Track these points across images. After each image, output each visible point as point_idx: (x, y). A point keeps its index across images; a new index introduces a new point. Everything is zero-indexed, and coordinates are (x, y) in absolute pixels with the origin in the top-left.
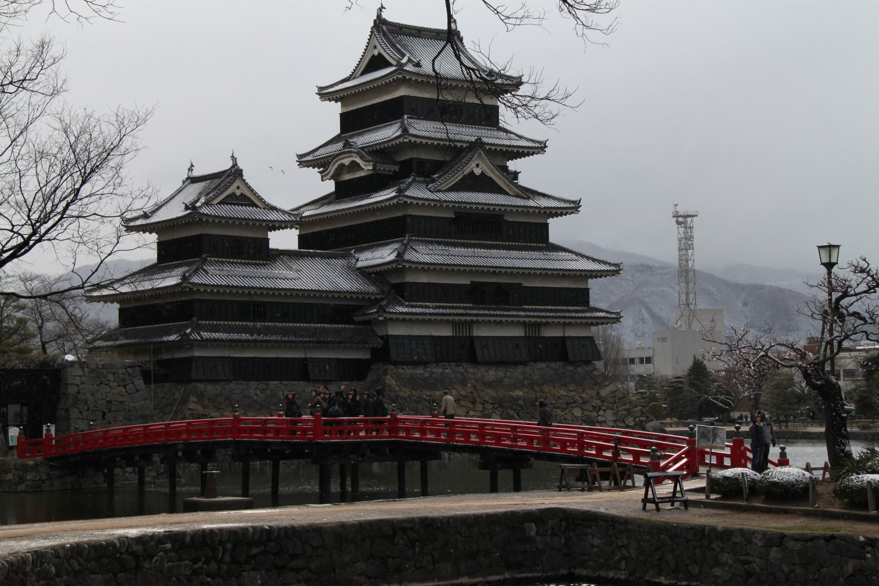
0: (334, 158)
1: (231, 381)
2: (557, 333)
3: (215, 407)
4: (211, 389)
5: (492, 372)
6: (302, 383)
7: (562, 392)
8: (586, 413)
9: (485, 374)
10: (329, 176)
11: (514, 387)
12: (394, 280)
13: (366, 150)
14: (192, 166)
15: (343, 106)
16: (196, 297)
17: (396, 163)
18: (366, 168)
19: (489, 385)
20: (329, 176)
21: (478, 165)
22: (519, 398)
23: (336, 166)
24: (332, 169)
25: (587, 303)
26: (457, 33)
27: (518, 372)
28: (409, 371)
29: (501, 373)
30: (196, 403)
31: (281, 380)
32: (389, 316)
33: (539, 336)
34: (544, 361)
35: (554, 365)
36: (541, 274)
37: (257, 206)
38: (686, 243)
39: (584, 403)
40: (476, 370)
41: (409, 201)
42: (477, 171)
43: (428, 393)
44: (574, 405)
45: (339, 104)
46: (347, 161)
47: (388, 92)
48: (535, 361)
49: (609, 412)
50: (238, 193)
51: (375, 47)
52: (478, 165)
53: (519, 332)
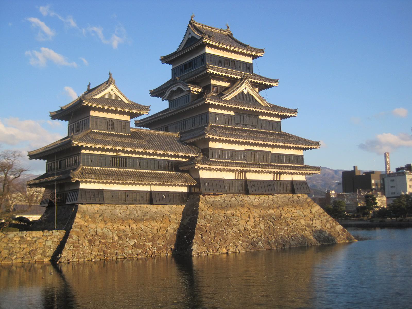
0: (168, 88)
5: (257, 200)
6: (149, 206)
9: (253, 201)
10: (166, 98)
12: (202, 147)
13: (186, 81)
14: (90, 84)
15: (173, 66)
18: (185, 90)
19: (256, 207)
20: (166, 98)
22: (272, 214)
23: (169, 92)
24: (167, 94)
25: (302, 163)
30: (80, 218)
31: (136, 204)
32: (200, 166)
33: (280, 180)
39: (305, 216)
42: (246, 92)
44: (300, 217)
45: (171, 65)
46: (175, 89)
47: (198, 53)
49: (318, 221)
51: (190, 34)
52: (245, 88)
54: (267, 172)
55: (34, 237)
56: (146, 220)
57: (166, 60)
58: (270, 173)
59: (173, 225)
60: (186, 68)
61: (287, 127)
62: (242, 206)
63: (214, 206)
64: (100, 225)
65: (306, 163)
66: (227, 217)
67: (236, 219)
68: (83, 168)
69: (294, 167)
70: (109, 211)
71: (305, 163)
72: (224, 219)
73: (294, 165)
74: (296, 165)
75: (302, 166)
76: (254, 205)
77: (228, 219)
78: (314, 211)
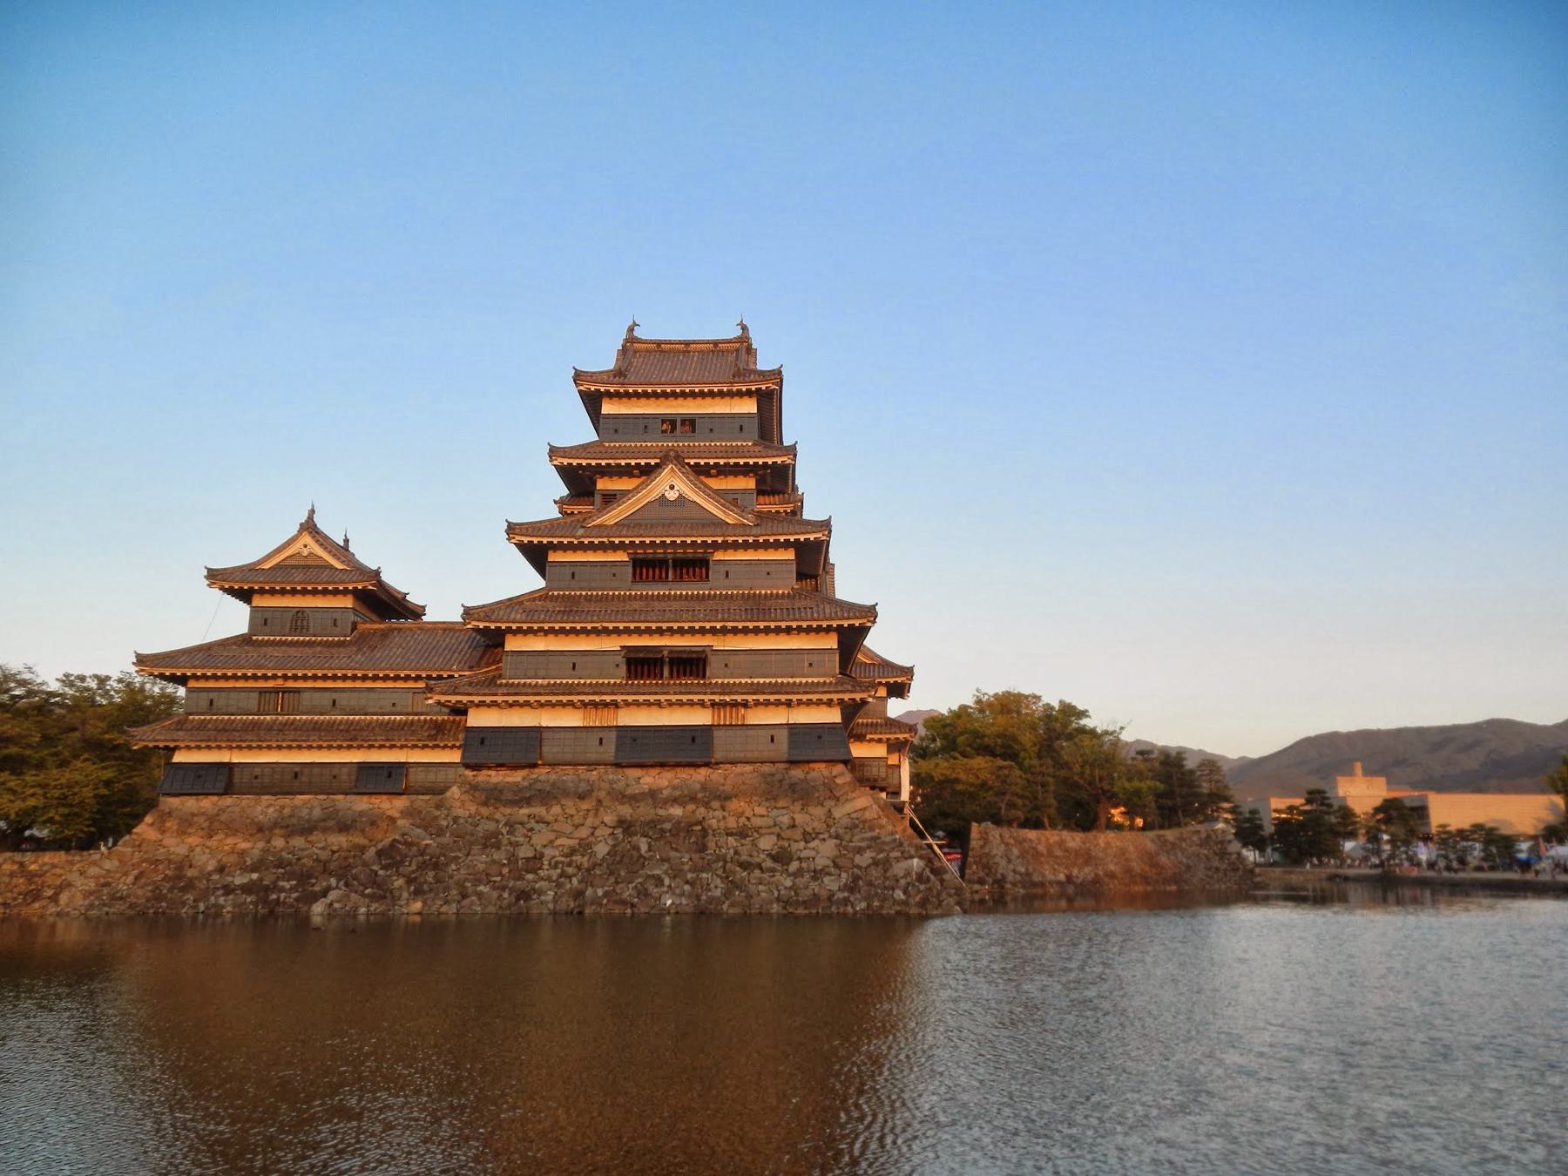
4: (190, 804)
7: (758, 810)
11: (675, 801)
21: (672, 487)
22: (668, 819)
28: (495, 777)
32: (443, 699)
42: (672, 496)
53: (702, 718)
56: (325, 830)
63: (493, 796)
70: (237, 809)
76: (629, 791)
78: (837, 813)
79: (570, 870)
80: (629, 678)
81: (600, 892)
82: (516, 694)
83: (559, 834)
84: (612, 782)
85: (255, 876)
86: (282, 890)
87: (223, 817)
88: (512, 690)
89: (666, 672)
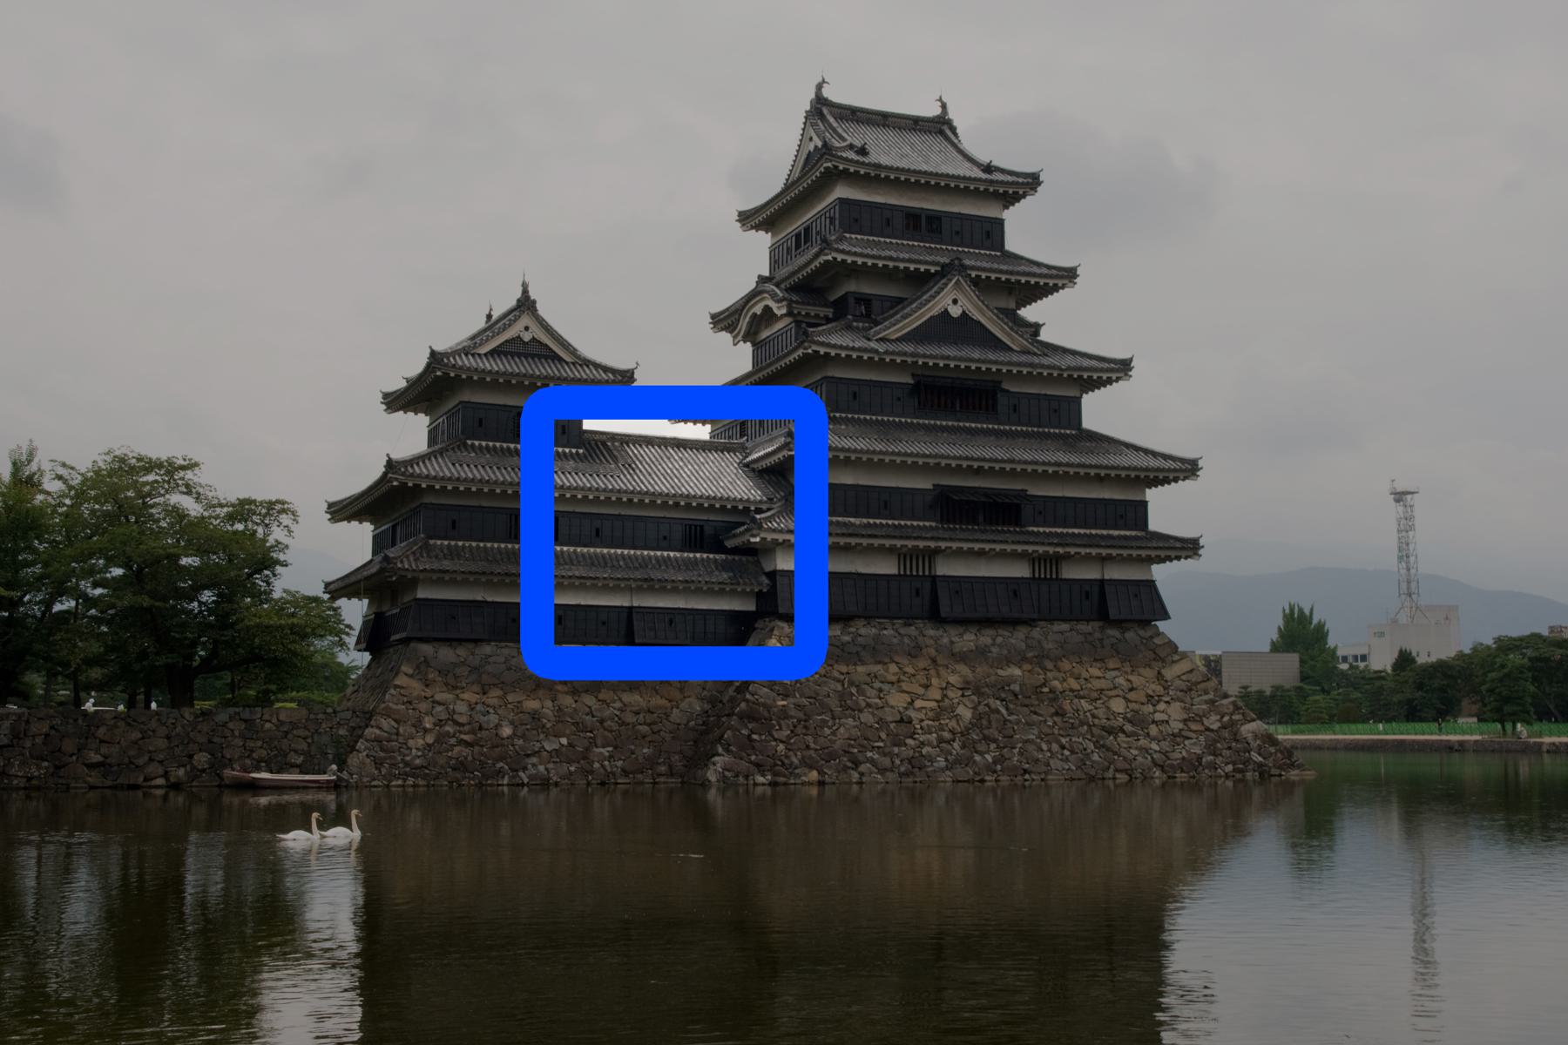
1: (488, 641)
2: (1091, 573)
3: (446, 684)
4: (446, 654)
5: (969, 636)
8: (1133, 706)
11: (1008, 661)
16: (428, 499)
17: (826, 306)
21: (955, 302)
22: (1011, 680)
26: (949, 123)
27: (1017, 638)
29: (985, 638)
30: (411, 676)
32: (770, 537)
34: (1065, 620)
35: (1084, 627)
36: (1056, 473)
37: (560, 359)
38: (1406, 525)
39: (1131, 690)
40: (940, 632)
41: (822, 351)
42: (955, 311)
43: (844, 669)
46: (758, 309)
48: (1051, 620)
50: (527, 337)
52: (955, 302)
53: (1021, 571)
54: (1003, 555)
55: (282, 723)
57: (747, 219)
58: (1023, 556)
59: (690, 704)
60: (798, 246)
61: (1100, 411)
62: (914, 652)
64: (465, 696)
65: (1158, 522)
66: (851, 683)
67: (880, 690)
68: (426, 545)
69: (1110, 537)
71: (1155, 524)
72: (840, 688)
73: (1099, 532)
74: (1116, 533)
75: (1139, 534)
77: (854, 690)
78: (1169, 673)
79: (946, 735)
80: (942, 521)
81: (989, 758)
82: (850, 535)
83: (919, 697)
84: (936, 639)
85: (564, 741)
86: (602, 759)
87: (489, 668)
88: (844, 531)
89: (981, 518)
